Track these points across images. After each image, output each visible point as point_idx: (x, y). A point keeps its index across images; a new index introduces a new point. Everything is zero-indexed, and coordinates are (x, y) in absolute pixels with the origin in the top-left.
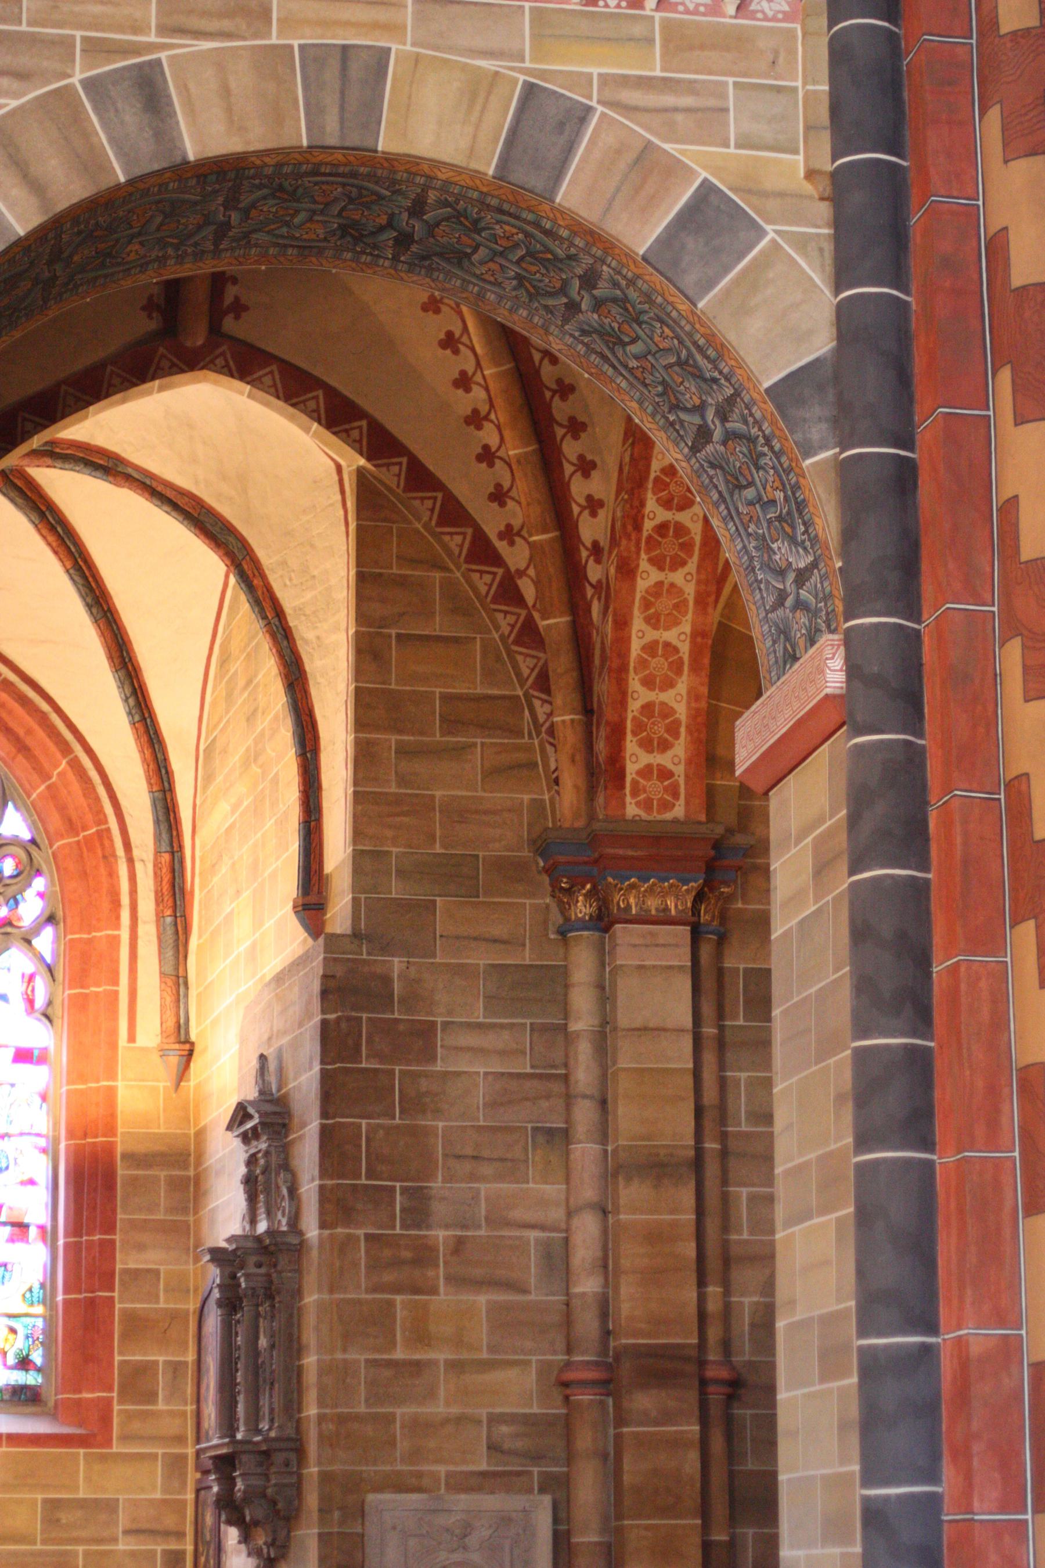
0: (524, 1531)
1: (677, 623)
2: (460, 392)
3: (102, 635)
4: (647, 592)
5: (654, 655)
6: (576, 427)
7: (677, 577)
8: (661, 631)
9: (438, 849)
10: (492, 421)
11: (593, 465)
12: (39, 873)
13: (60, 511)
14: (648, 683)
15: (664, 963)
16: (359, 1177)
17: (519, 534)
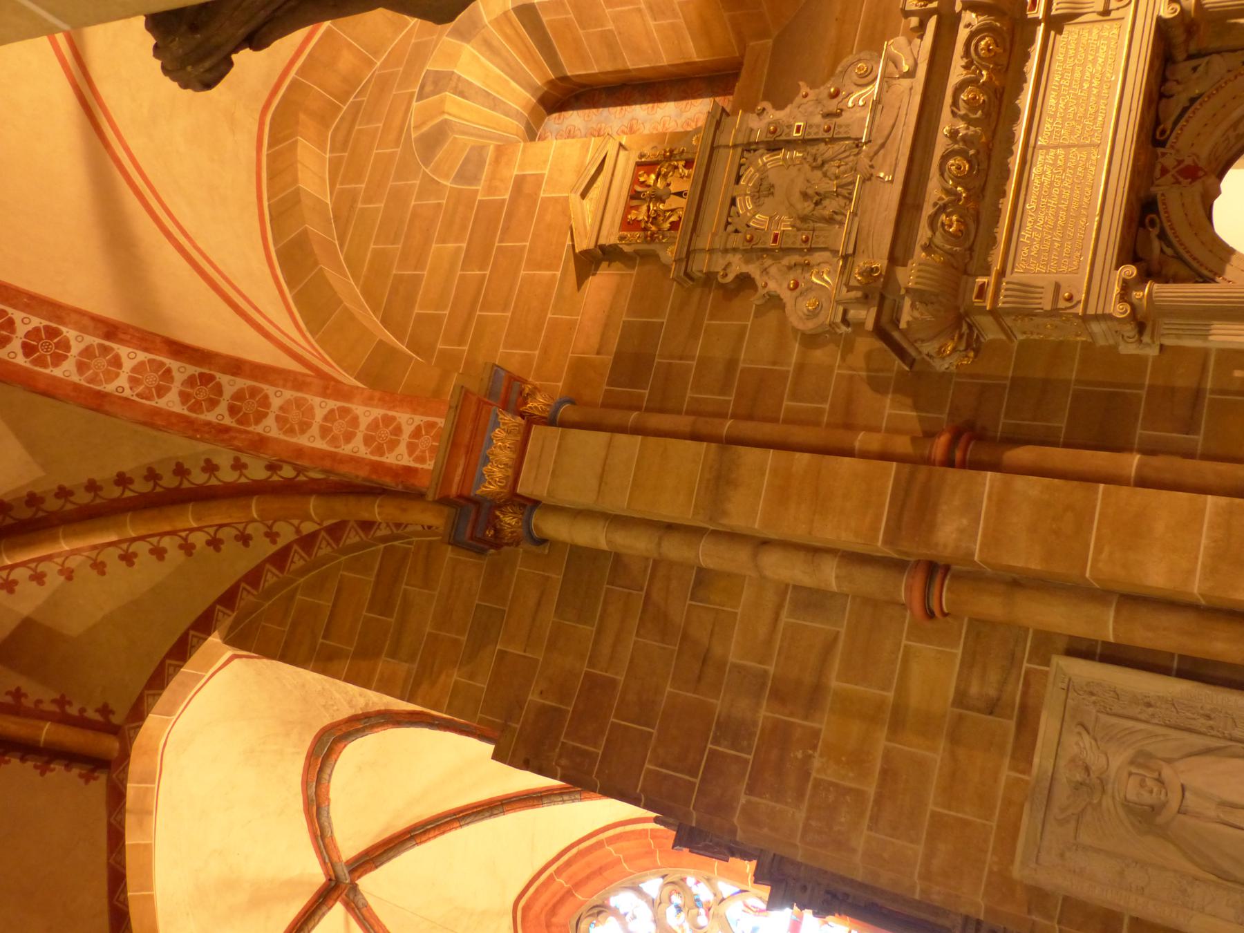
0: (1092, 694)
1: (311, 408)
2: (167, 556)
3: (514, 810)
4: (280, 429)
5: (330, 430)
6: (181, 471)
7: (276, 403)
8: (314, 422)
9: (464, 639)
10: (187, 535)
11: (208, 461)
12: (684, 880)
13: (415, 824)
14: (349, 437)
15: (555, 451)
16: (694, 784)
17: (270, 527)
